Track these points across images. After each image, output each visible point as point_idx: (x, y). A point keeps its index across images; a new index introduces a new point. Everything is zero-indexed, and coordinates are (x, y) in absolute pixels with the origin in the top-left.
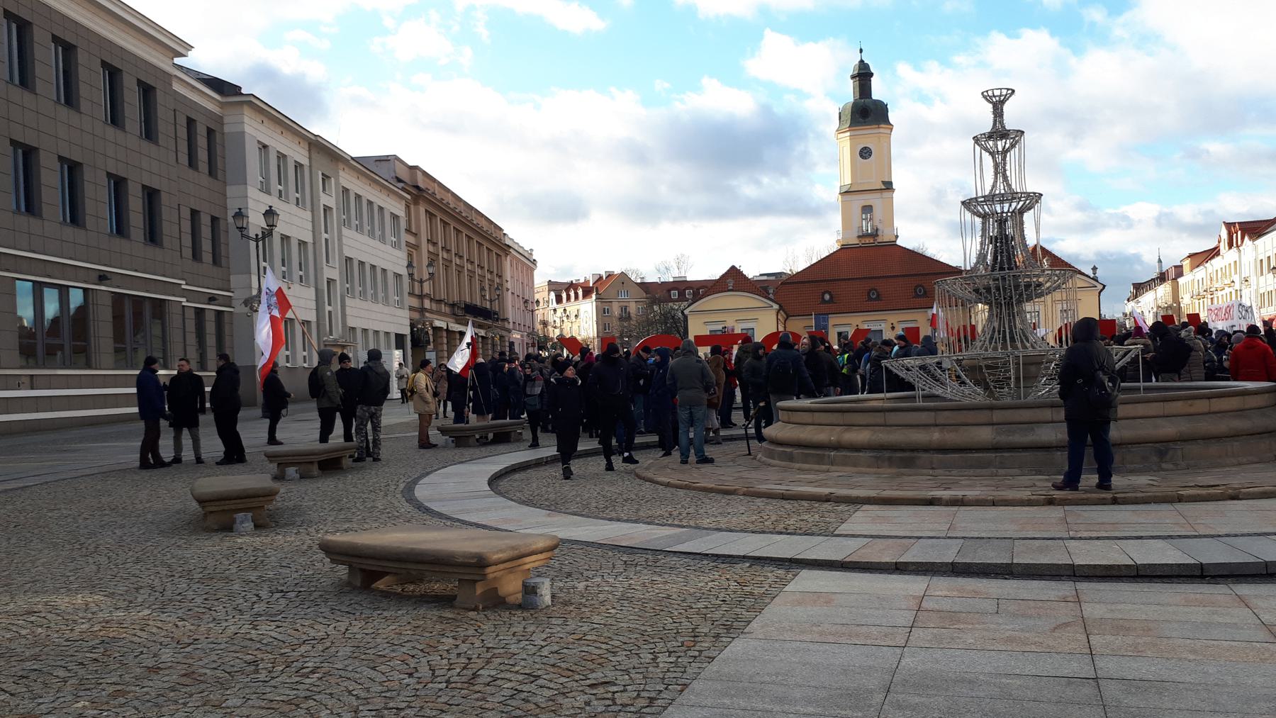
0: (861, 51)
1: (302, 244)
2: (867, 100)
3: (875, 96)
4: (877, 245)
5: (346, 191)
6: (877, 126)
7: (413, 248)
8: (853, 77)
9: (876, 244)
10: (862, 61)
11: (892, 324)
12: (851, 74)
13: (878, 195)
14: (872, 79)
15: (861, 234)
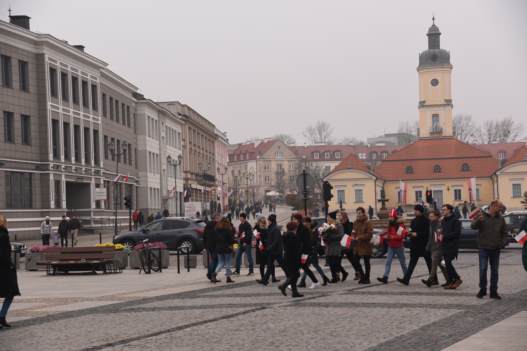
0: (433, 19)
1: (157, 155)
2: (436, 50)
3: (442, 47)
4: (441, 139)
5: (166, 126)
6: (442, 67)
7: (184, 147)
8: (428, 35)
9: (441, 137)
10: (434, 25)
11: (448, 187)
12: (427, 32)
13: (442, 108)
14: (440, 36)
15: (432, 131)
